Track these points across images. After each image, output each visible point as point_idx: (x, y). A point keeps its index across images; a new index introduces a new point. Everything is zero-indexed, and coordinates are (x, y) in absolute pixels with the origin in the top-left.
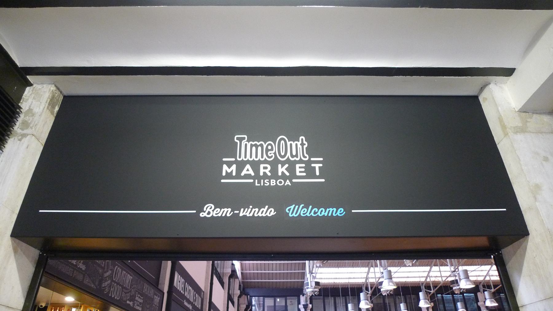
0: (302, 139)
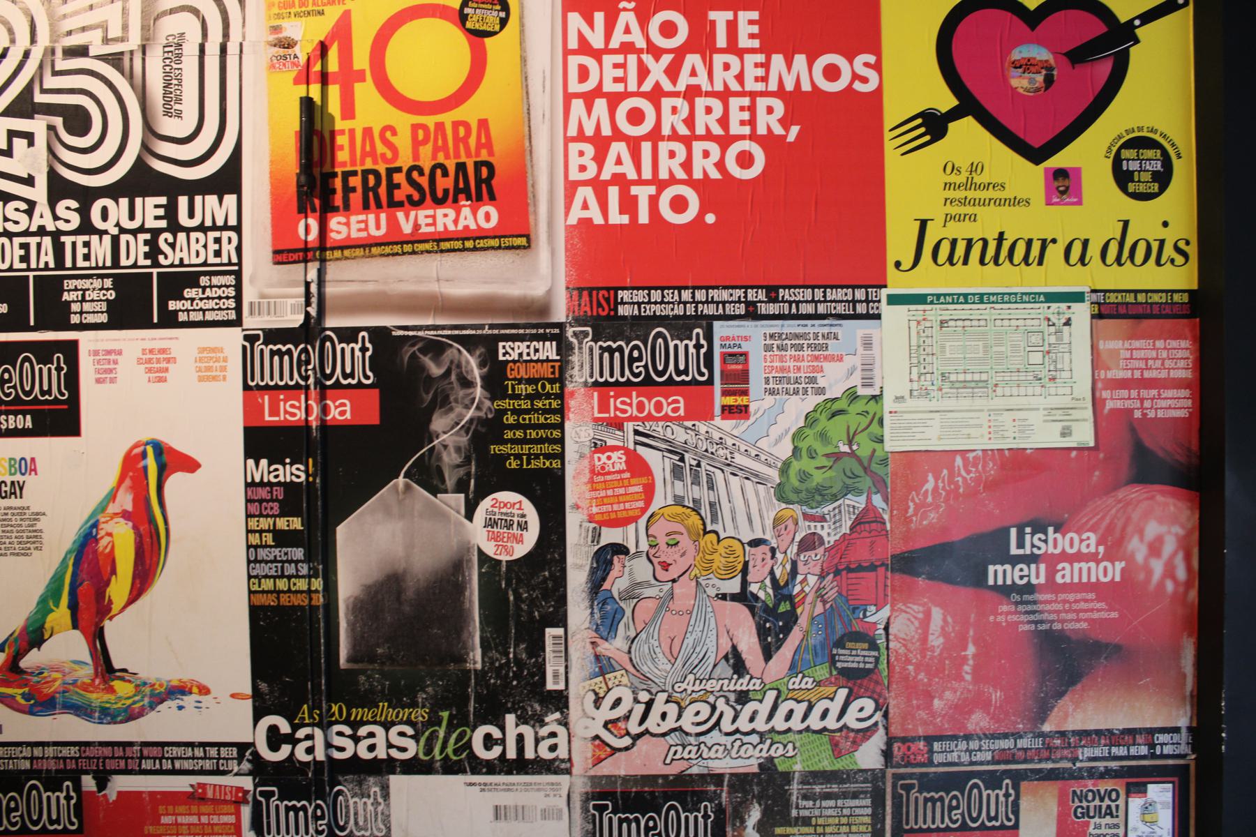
0: (363, 337)
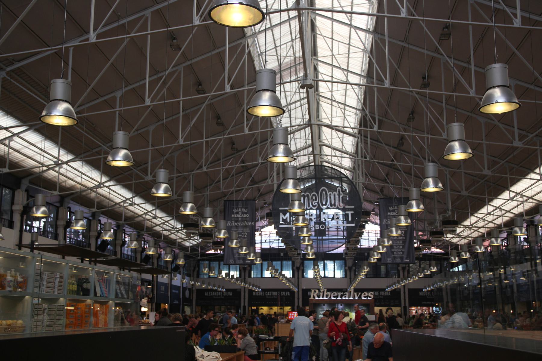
0: (339, 190)
